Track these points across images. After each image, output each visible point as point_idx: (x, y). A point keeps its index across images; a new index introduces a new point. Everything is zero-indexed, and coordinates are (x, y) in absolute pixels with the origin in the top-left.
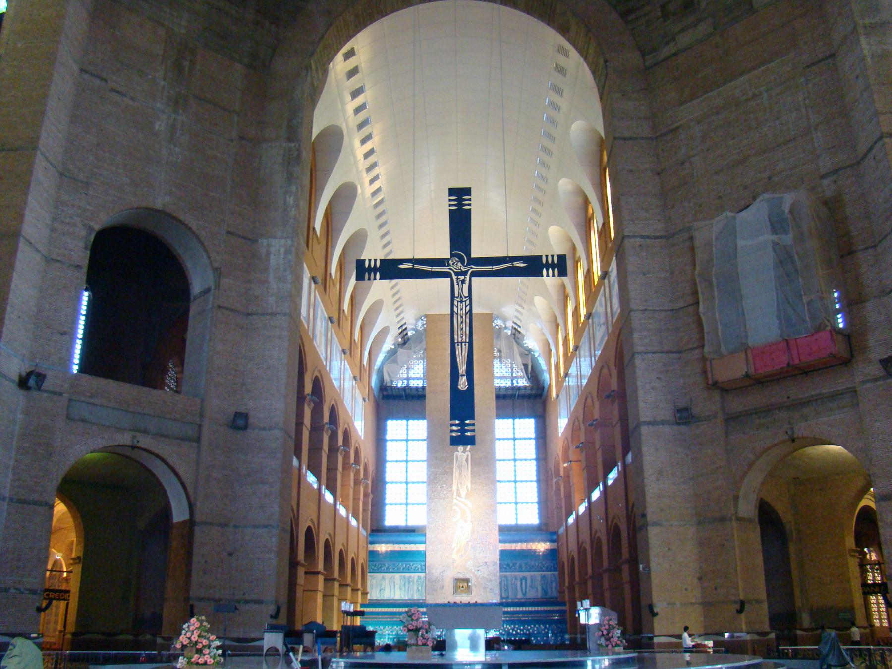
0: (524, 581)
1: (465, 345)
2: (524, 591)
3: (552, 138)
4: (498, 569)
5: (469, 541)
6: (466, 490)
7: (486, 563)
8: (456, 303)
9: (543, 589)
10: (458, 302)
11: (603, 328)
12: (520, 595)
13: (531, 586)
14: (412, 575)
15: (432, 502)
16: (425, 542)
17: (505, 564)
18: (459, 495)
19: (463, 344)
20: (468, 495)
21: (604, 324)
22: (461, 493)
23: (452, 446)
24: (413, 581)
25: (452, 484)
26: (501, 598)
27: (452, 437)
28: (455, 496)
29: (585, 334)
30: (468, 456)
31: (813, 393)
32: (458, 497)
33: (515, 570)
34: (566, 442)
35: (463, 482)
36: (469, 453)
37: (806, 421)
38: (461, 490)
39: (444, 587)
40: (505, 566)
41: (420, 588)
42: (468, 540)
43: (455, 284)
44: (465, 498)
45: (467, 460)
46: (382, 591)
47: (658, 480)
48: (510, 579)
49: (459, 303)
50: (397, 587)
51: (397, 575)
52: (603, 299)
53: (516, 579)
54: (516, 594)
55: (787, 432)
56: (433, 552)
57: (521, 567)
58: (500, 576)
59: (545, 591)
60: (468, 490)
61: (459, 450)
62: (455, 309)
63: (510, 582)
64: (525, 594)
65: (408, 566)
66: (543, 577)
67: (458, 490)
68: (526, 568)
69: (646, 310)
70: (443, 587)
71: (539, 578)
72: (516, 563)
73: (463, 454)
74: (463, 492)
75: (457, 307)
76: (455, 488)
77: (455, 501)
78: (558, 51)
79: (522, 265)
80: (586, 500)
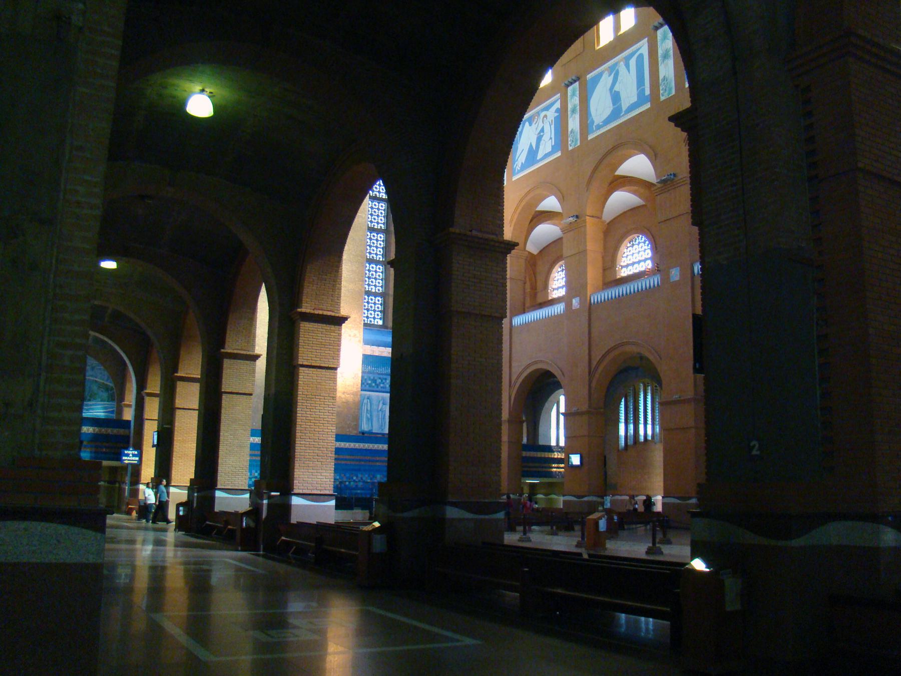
17: (370, 379)
23: (691, 226)
48: (374, 402)
63: (375, 407)
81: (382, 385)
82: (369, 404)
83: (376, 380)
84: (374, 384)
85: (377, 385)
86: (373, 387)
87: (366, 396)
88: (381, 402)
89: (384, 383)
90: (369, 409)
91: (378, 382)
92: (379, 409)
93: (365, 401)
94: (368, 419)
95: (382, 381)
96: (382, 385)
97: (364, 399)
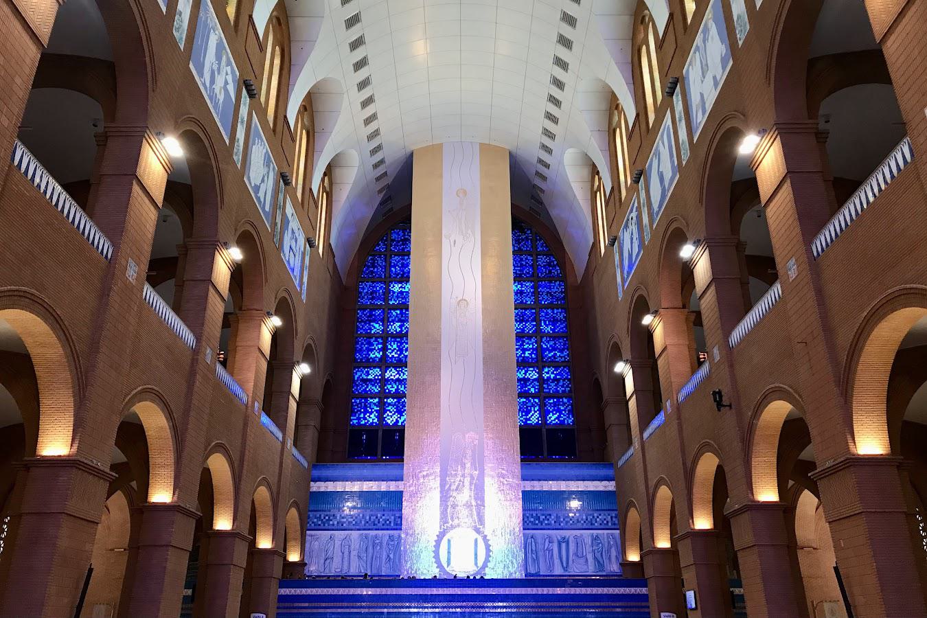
0: (564, 545)
2: (565, 565)
9: (595, 558)
12: (558, 570)
13: (576, 554)
14: (380, 532)
24: (381, 543)
40: (532, 520)
41: (392, 556)
46: (328, 561)
48: (539, 541)
50: (354, 553)
51: (355, 534)
54: (551, 566)
59: (599, 564)
63: (540, 547)
64: (565, 569)
65: (372, 520)
66: (595, 539)
71: (588, 541)
81: (546, 522)
82: (533, 543)
84: (537, 522)
88: (547, 540)
89: (548, 520)
90: (534, 549)
93: (529, 541)
95: (546, 517)
96: (546, 522)
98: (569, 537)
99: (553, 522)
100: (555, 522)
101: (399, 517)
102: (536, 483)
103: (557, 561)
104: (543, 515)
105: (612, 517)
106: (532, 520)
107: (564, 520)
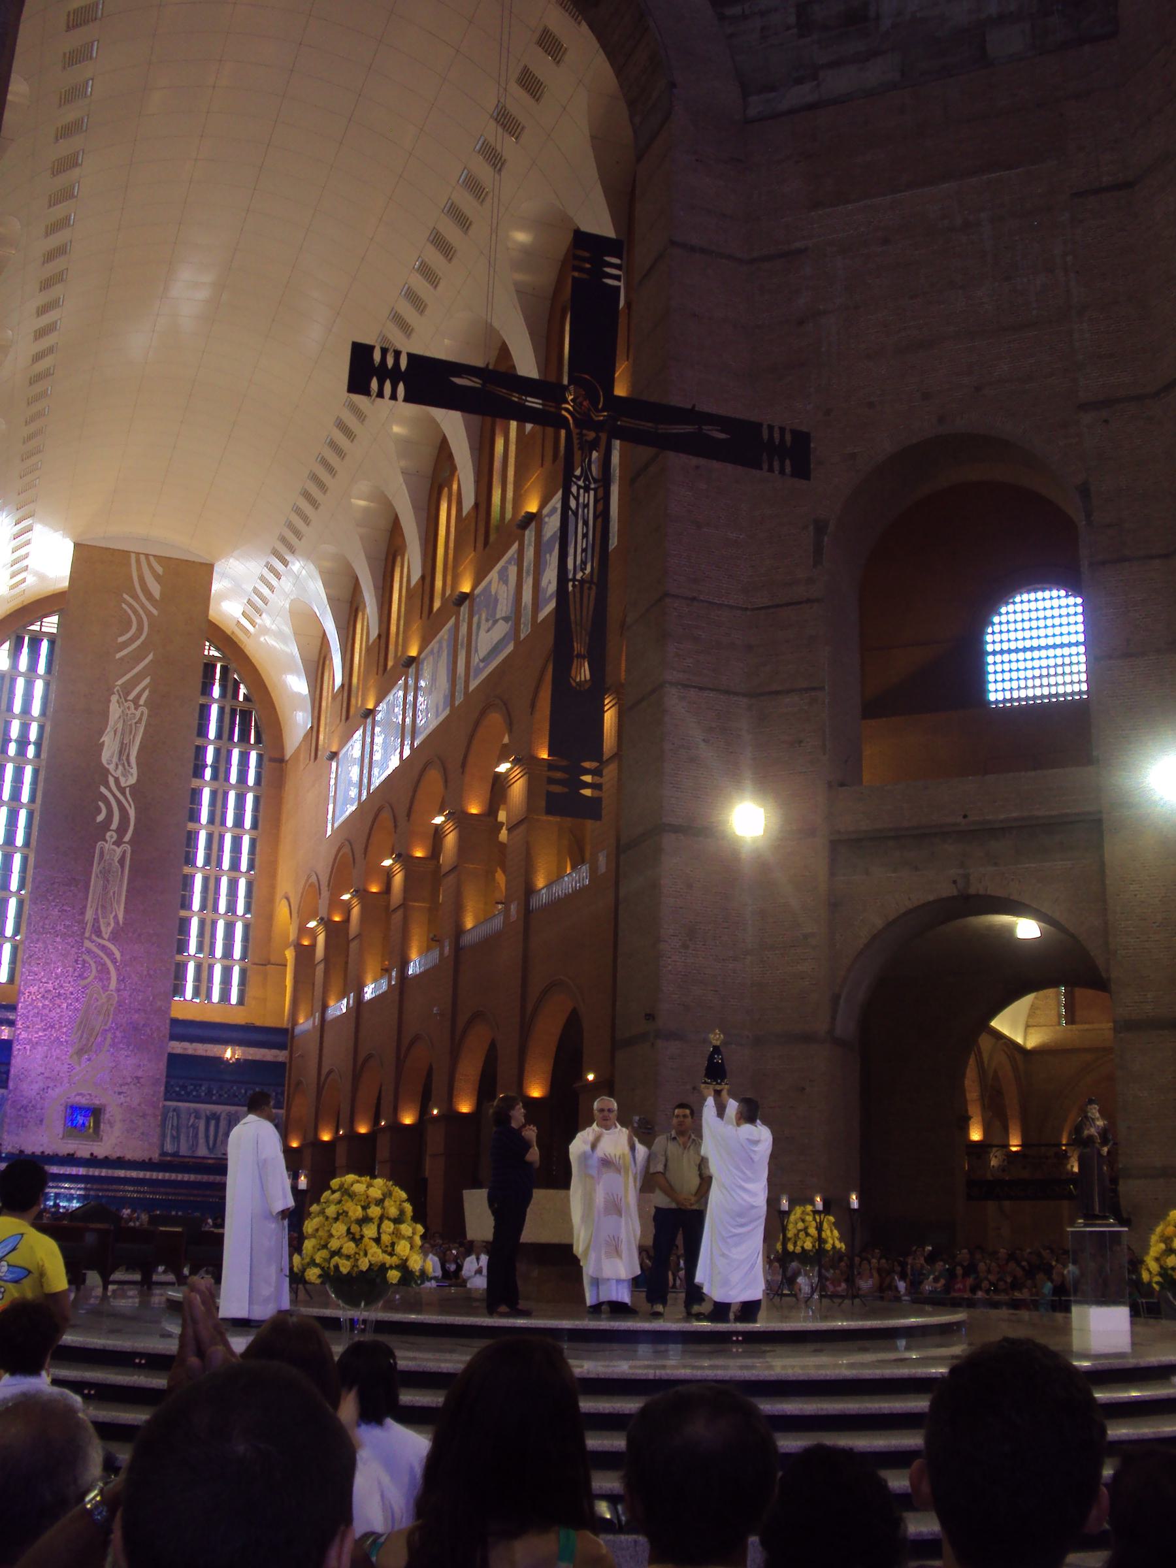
0: (213, 1123)
1: (590, 588)
3: (463, 222)
4: (162, 1094)
5: (109, 1030)
6: (112, 924)
7: (137, 1078)
8: (574, 489)
10: (579, 487)
11: (502, 629)
12: (202, 1151)
15: (38, 940)
16: (11, 1023)
18: (98, 933)
19: (587, 585)
20: (114, 938)
21: (506, 619)
22: (103, 929)
25: (85, 907)
26: (163, 1154)
27: (549, 795)
28: (87, 934)
29: (444, 633)
30: (124, 852)
31: (1015, 815)
32: (94, 937)
33: (198, 1100)
34: (346, 849)
35: (109, 908)
36: (128, 848)
37: (996, 864)
38: (101, 920)
39: (44, 1122)
40: (178, 1089)
42: (107, 1028)
43: (576, 447)
44: (109, 940)
45: (122, 861)
47: (685, 946)
49: (582, 491)
52: (513, 570)
53: (197, 1117)
55: (955, 882)
56: (28, 1047)
57: (209, 1092)
58: (164, 1106)
60: (117, 923)
61: (108, 838)
62: (573, 504)
64: (211, 1150)
67: (96, 920)
68: (221, 1096)
69: (694, 599)
70: (41, 1121)
72: (201, 1086)
73: (114, 847)
74: (106, 932)
75: (577, 499)
76: (89, 915)
77: (87, 944)
78: (540, 43)
79: (723, 436)
80: (394, 974)
81: (194, 1093)
82: (175, 1118)
83: (186, 1087)
84: (183, 1093)
85: (189, 1094)
86: (183, 1095)
87: (172, 1109)
88: (193, 1115)
89: (197, 1091)
90: (175, 1124)
91: (189, 1090)
92: (190, 1124)
93: (170, 1114)
94: (173, 1137)
95: (195, 1088)
97: (168, 1112)
98: (221, 1113)
99: (203, 1094)
100: (206, 1094)
101: (4, 1073)
102: (186, 1045)
103: (202, 1141)
104: (192, 1085)
105: (277, 1094)
106: (178, 1089)
107: (217, 1092)
